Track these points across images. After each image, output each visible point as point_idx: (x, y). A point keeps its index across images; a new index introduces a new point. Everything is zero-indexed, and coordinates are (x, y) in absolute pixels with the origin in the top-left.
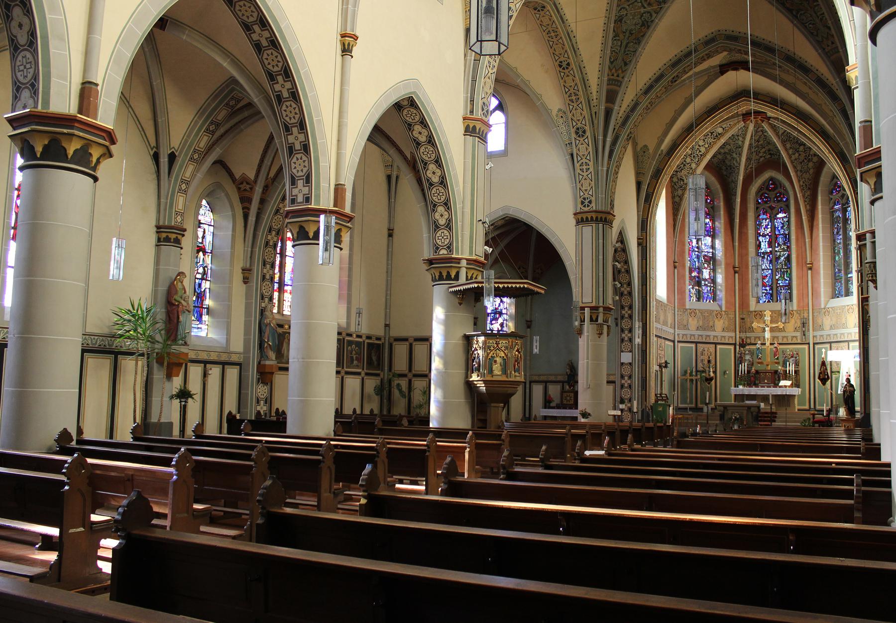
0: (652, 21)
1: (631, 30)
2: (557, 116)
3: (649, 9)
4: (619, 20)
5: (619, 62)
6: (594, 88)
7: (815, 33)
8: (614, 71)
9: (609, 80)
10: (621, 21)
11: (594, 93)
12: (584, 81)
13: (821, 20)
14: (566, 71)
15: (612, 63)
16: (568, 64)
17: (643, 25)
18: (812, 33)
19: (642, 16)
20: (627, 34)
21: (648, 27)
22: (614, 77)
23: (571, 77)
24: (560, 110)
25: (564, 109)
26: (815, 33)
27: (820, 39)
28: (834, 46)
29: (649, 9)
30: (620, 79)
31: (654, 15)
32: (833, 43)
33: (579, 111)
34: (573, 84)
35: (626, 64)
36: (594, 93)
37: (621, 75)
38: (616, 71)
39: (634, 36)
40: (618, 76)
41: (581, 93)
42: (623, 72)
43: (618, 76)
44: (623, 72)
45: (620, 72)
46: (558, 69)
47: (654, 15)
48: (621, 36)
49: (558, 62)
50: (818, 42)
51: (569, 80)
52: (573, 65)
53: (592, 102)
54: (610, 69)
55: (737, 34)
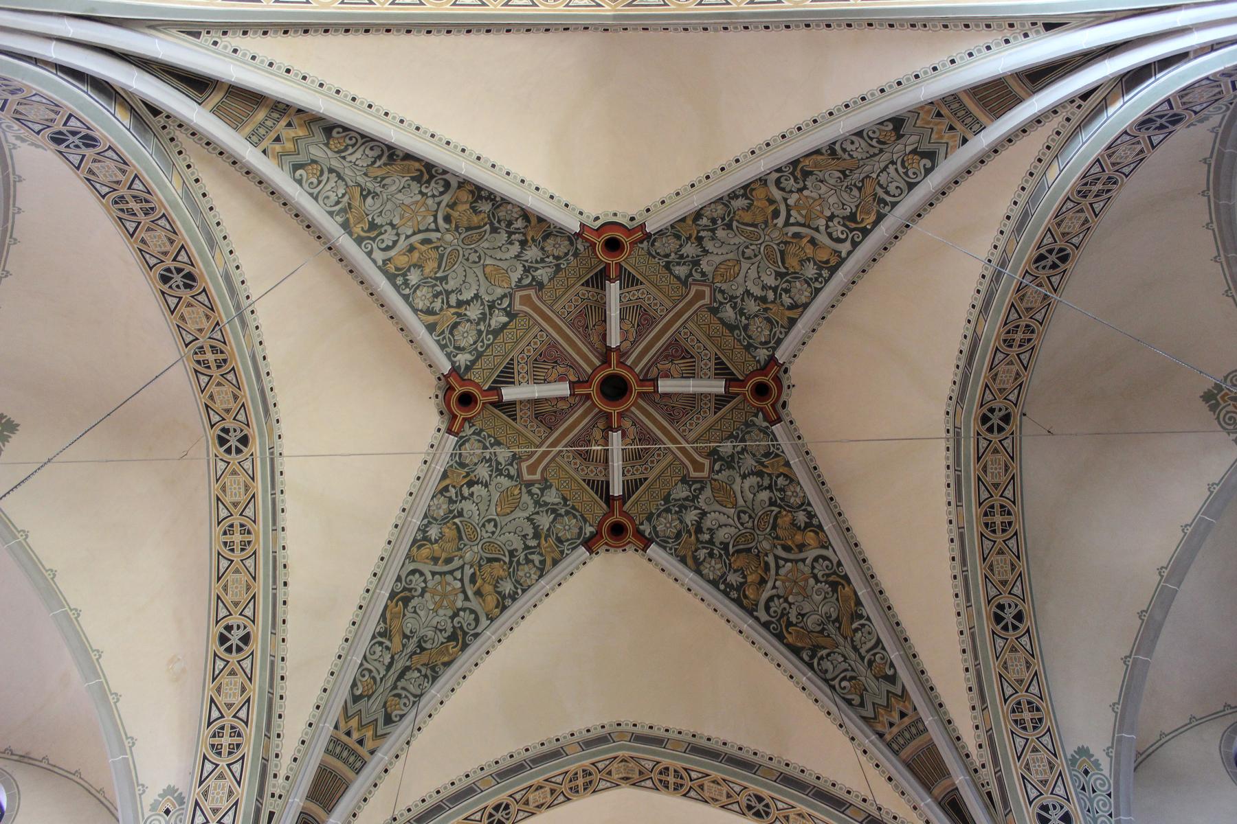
0: (476, 635)
1: (422, 639)
2: (153, 808)
3: (474, 603)
4: (402, 597)
5: (373, 707)
6: (288, 747)
7: (857, 700)
8: (354, 723)
9: (334, 741)
10: (406, 601)
11: (286, 760)
12: (271, 714)
13: (870, 663)
14: (234, 658)
15: (356, 699)
16: (246, 639)
17: (453, 637)
18: (849, 702)
19: (456, 615)
20: (412, 646)
21: (465, 646)
22: (351, 742)
23: (240, 678)
24: (170, 791)
25: (182, 788)
26: (857, 700)
27: (869, 713)
28: (907, 720)
29: (474, 603)
30: (363, 751)
31: (484, 622)
32: (903, 715)
33: (229, 781)
34: (238, 700)
35: (388, 720)
36: (286, 760)
37: (370, 744)
38: (361, 726)
39: (424, 658)
40: (361, 742)
41: (250, 733)
42: (376, 736)
43: (361, 742)
44: (376, 736)
45: (369, 734)
46: (215, 646)
47: (484, 622)
48: (397, 639)
49: (220, 628)
50: (864, 719)
51: (231, 686)
52: (256, 645)
53: (270, 780)
54: (346, 715)
55: (662, 733)
